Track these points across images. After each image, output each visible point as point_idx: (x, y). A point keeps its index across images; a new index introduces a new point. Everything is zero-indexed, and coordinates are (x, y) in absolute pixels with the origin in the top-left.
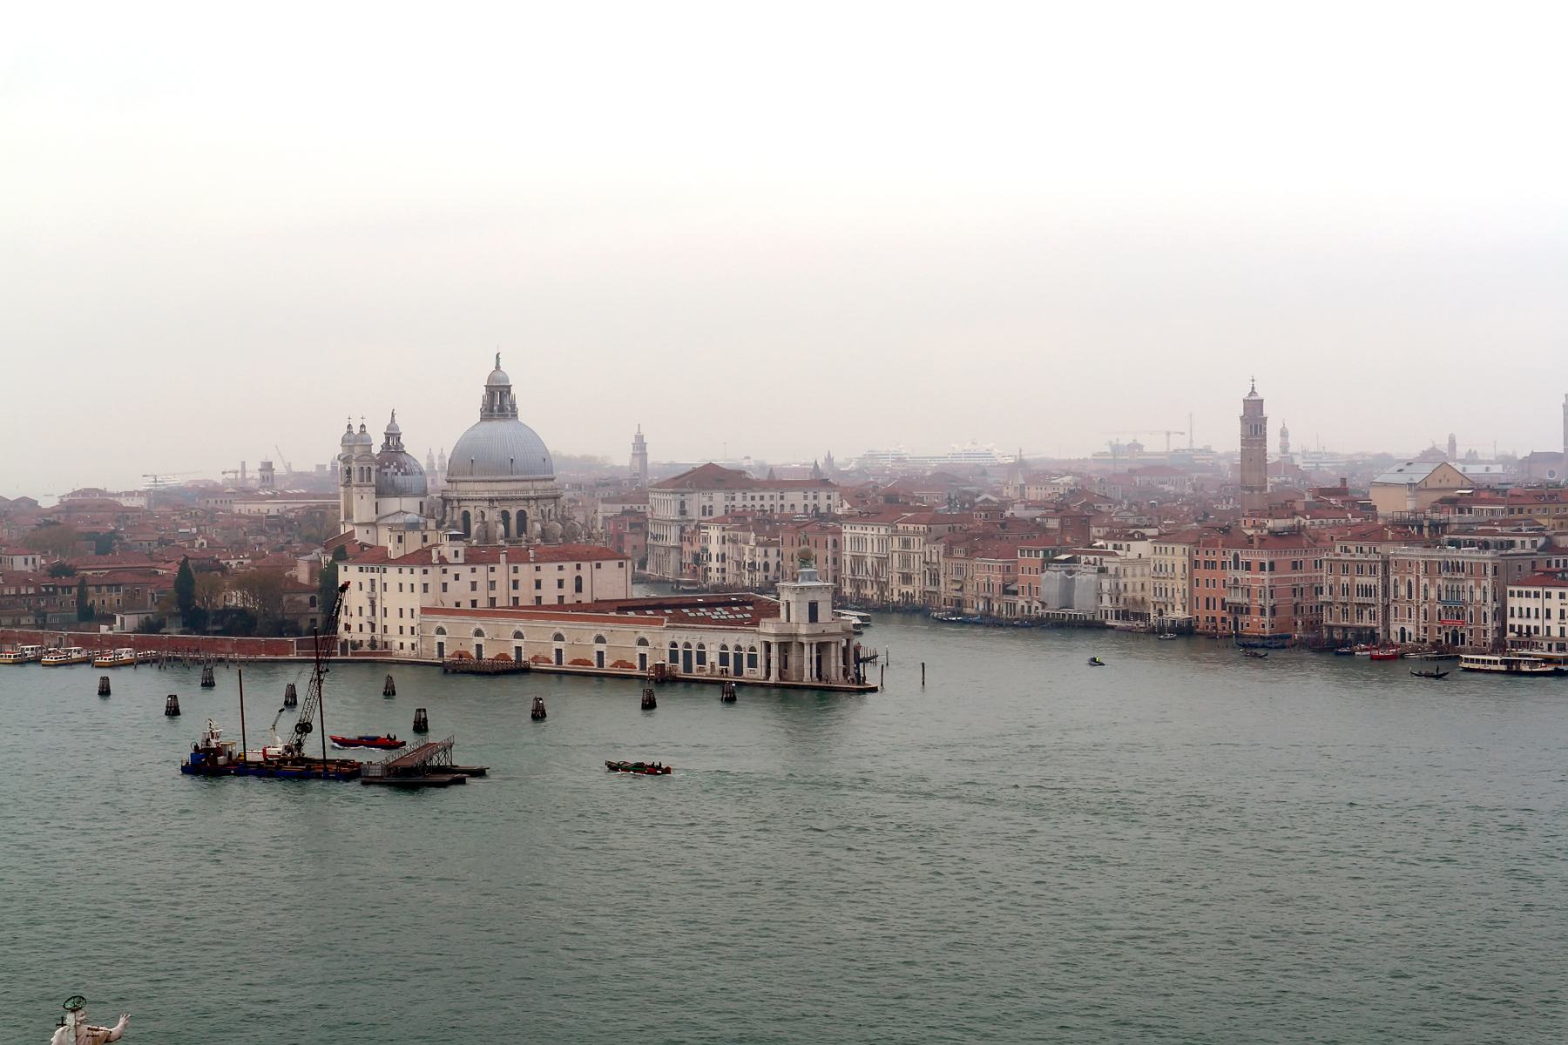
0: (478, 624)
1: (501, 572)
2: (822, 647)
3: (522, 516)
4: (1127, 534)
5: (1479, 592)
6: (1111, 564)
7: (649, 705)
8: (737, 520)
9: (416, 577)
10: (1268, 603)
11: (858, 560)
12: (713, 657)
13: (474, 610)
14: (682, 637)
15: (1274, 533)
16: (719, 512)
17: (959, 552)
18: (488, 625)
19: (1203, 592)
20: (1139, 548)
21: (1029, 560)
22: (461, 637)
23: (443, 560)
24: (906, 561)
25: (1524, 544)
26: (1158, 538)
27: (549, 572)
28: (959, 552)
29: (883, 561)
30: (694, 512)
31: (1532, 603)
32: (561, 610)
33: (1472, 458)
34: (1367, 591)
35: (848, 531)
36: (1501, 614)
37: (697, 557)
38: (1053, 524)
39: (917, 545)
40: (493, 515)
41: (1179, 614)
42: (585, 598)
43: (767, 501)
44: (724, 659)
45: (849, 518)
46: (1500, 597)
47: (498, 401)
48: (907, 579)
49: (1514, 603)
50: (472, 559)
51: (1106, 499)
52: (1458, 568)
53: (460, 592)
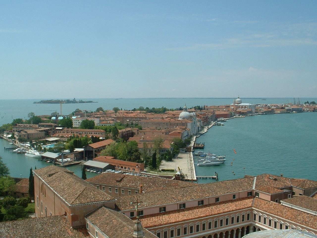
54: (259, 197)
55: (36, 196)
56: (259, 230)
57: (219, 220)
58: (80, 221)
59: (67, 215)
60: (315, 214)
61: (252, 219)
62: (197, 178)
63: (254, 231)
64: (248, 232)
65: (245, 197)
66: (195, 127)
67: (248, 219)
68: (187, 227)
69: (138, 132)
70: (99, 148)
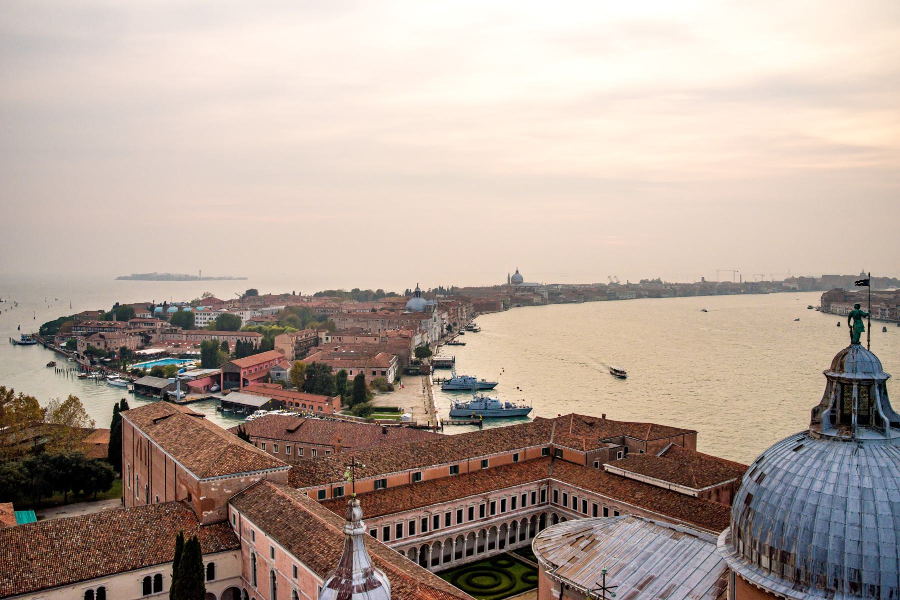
54: (564, 458)
55: (127, 463)
56: (564, 520)
57: (488, 502)
58: (219, 511)
59: (193, 500)
60: (667, 487)
61: (551, 500)
62: (442, 424)
63: (555, 521)
64: (543, 527)
65: (536, 458)
66: (435, 328)
67: (543, 500)
68: (428, 517)
69: (327, 339)
70: (267, 364)
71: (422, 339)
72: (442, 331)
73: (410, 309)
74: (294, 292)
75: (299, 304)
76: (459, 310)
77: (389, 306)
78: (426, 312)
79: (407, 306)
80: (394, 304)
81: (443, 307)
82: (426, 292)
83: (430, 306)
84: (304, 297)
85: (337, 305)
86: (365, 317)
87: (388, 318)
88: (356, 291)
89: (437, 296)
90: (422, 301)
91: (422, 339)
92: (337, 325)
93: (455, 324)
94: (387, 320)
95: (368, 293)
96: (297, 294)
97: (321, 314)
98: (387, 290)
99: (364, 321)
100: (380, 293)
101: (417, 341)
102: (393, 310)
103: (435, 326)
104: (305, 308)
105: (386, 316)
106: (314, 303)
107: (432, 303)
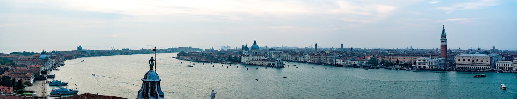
0: (253, 61)
1: (255, 57)
2: (280, 64)
3: (257, 52)
4: (306, 55)
5: (334, 60)
6: (304, 57)
7: (266, 68)
8: (274, 53)
9: (248, 57)
10: (317, 60)
11: (284, 56)
12: (271, 64)
13: (252, 60)
14: (269, 63)
15: (317, 55)
16: (273, 52)
17: (292, 56)
18: (253, 61)
19: (311, 60)
20: (307, 56)
21: (297, 57)
22: (251, 62)
23: (250, 56)
24: (288, 56)
25: (338, 56)
26: (308, 55)
27: (259, 57)
28: (292, 56)
29: (286, 57)
30: (271, 52)
31: (338, 61)
32: (260, 60)
33: (334, 49)
34: (325, 60)
35: (283, 54)
36: (335, 62)
37: (271, 56)
38: (300, 54)
39: (289, 55)
40: (254, 52)
41: (310, 61)
42: (261, 59)
43: (276, 51)
44: (272, 64)
45: (283, 53)
46: (335, 60)
47: (255, 43)
48: (288, 58)
49: (336, 61)
50: (252, 56)
51: (304, 52)
52: (332, 58)
53: (251, 58)
71: (45, 68)
72: (52, 65)
73: (41, 58)
74: (3, 53)
75: (4, 57)
76: (59, 59)
77: (35, 57)
78: (47, 59)
79: (40, 57)
80: (36, 57)
81: (53, 58)
82: (49, 52)
83: (48, 57)
84: (6, 54)
85: (17, 57)
86: (26, 61)
87: (33, 61)
88: (24, 52)
89: (53, 54)
90: (45, 56)
91: (45, 68)
92: (15, 63)
93: (57, 63)
94: (33, 62)
95: (29, 53)
96: (4, 53)
97: (11, 60)
98: (35, 52)
99: (25, 62)
100: (33, 53)
101: (43, 69)
102: (35, 59)
103: (49, 64)
104: (6, 58)
105: (33, 61)
106: (9, 56)
107: (48, 56)
